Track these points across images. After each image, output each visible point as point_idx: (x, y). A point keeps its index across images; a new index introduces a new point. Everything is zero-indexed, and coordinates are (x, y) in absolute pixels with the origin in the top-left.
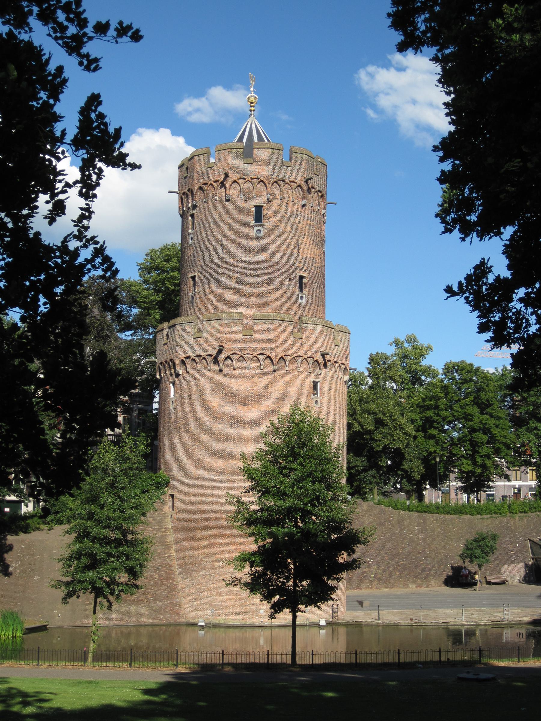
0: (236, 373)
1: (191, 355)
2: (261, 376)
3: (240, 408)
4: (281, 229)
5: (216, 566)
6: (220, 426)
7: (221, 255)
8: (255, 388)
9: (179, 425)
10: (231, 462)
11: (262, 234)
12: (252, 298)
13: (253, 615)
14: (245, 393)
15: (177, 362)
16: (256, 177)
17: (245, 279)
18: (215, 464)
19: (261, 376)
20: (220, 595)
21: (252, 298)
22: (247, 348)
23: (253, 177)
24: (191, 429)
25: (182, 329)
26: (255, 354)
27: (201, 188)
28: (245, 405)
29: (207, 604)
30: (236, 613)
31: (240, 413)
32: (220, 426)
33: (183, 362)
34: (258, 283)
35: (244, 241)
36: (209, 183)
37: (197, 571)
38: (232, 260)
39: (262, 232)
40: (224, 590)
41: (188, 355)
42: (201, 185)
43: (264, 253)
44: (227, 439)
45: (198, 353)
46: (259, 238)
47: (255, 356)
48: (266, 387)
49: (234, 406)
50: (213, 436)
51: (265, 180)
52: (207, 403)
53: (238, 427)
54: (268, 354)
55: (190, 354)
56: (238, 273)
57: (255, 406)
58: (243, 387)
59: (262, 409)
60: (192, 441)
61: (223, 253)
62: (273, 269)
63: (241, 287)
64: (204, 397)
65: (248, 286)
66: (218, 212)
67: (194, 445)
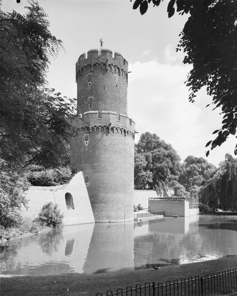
0: (114, 134)
22: (118, 125)
26: (120, 128)
27: (95, 64)
28: (117, 146)
33: (92, 128)
47: (120, 129)
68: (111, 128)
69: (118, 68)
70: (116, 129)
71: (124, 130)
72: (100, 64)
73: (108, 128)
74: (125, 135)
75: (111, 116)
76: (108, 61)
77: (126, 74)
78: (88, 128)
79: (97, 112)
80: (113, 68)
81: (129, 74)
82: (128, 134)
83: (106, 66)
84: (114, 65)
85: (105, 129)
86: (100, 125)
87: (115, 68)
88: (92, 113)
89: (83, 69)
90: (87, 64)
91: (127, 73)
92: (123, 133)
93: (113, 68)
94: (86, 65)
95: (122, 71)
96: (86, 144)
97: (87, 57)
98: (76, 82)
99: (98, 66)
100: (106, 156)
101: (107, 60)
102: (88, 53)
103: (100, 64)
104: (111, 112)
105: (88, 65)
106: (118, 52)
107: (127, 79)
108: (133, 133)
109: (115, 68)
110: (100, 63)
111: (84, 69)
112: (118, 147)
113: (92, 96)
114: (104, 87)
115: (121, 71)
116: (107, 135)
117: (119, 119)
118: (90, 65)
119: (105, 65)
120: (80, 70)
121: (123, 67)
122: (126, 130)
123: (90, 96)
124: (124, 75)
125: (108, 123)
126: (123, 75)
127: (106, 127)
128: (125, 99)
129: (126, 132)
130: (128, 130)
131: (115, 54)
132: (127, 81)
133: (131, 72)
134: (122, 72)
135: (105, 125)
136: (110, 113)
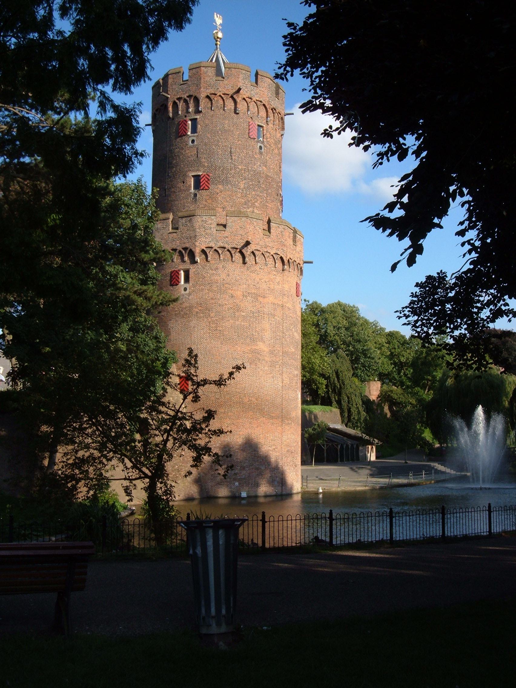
0: (257, 267)
1: (213, 246)
2: (275, 273)
3: (261, 299)
4: (273, 150)
6: (244, 314)
7: (230, 161)
8: (271, 283)
9: (196, 310)
10: (253, 347)
12: (256, 204)
15: (197, 251)
16: (260, 100)
17: (251, 187)
18: (239, 349)
19: (275, 273)
21: (256, 204)
22: (266, 247)
23: (257, 99)
24: (212, 315)
25: (202, 221)
26: (272, 253)
27: (208, 97)
28: (264, 297)
31: (260, 304)
32: (244, 314)
35: (250, 153)
36: (218, 94)
38: (240, 167)
41: (210, 245)
42: (209, 94)
43: (264, 168)
44: (250, 325)
45: (222, 245)
48: (278, 283)
49: (256, 297)
50: (237, 323)
51: (266, 105)
53: (258, 316)
55: (212, 244)
56: (245, 179)
58: (262, 281)
59: (276, 303)
60: (213, 326)
61: (232, 159)
62: (270, 183)
63: (248, 193)
64: (226, 285)
65: (253, 193)
66: (227, 122)
67: (216, 330)
68: (248, 253)
77: (282, 118)
80: (252, 105)
81: (286, 118)
84: (254, 99)
90: (187, 95)
93: (252, 105)
96: (183, 292)
101: (239, 89)
112: (266, 300)
113: (198, 170)
115: (270, 111)
122: (285, 259)
123: (193, 171)
129: (286, 261)
130: (288, 258)
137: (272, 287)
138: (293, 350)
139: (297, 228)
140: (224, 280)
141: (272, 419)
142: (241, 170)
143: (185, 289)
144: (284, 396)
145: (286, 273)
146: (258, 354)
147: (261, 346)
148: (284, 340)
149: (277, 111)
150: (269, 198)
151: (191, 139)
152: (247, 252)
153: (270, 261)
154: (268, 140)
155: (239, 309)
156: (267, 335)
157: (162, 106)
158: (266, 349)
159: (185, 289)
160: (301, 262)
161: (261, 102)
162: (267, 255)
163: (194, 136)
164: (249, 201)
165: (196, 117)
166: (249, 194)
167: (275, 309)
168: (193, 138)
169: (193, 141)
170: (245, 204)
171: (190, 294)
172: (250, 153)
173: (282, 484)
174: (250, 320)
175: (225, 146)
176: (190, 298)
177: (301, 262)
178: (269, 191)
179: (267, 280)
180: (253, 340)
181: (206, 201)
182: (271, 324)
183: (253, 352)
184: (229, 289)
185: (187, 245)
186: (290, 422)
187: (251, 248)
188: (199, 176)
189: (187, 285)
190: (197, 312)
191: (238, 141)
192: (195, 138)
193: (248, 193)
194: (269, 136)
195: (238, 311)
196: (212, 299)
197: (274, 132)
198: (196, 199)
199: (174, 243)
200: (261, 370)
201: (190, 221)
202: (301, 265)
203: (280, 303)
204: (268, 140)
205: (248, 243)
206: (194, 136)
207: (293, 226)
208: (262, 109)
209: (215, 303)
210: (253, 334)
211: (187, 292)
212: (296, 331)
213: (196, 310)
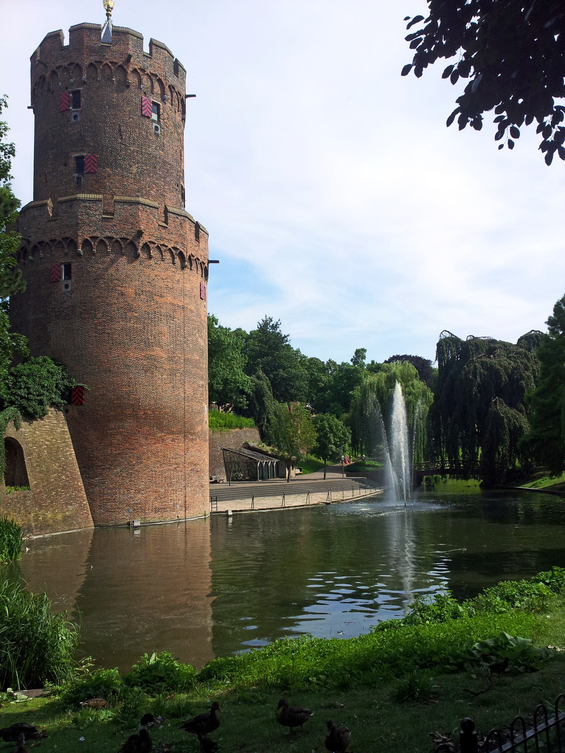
0: (152, 262)
1: (99, 235)
2: (174, 270)
4: (172, 133)
5: (134, 462)
6: (137, 315)
8: (169, 280)
9: (80, 310)
11: (159, 132)
13: (171, 511)
14: (161, 284)
16: (155, 73)
17: (145, 172)
18: (132, 354)
20: (139, 492)
22: (162, 238)
23: (152, 72)
24: (98, 316)
26: (170, 247)
27: (91, 65)
28: (161, 296)
29: (123, 504)
30: (156, 510)
31: (157, 304)
32: (137, 315)
33: (86, 243)
34: (157, 180)
35: (144, 133)
36: (104, 63)
37: (110, 469)
39: (159, 130)
40: (143, 486)
41: (95, 235)
46: (157, 135)
47: (170, 249)
48: (178, 281)
52: (120, 288)
54: (181, 249)
55: (97, 234)
56: (138, 163)
57: (170, 299)
61: (122, 138)
62: (168, 170)
63: (142, 179)
65: (148, 179)
68: (141, 245)
69: (160, 81)
70: (158, 247)
71: (181, 255)
72: (107, 64)
73: (133, 245)
74: (183, 267)
75: (142, 215)
76: (132, 60)
77: (182, 99)
78: (73, 243)
79: (101, 196)
80: (145, 79)
81: (188, 100)
82: (191, 265)
83: (125, 72)
84: (148, 71)
85: (123, 246)
86: (109, 235)
87: (151, 80)
88: (84, 201)
89: (54, 73)
91: (184, 98)
92: (177, 260)
93: (145, 79)
94: (66, 64)
95: (171, 91)
96: (64, 289)
97: (66, 42)
98: (29, 108)
99: (103, 71)
100: (129, 325)
101: (130, 57)
102: (70, 31)
103: (107, 64)
104: (141, 200)
105: (68, 65)
106: (160, 38)
107: (184, 112)
108: (204, 264)
109: (151, 80)
110: (108, 63)
111: (59, 73)
113: (82, 151)
114: (120, 130)
116: (130, 262)
117: (166, 222)
118: (78, 67)
119: (122, 69)
120: (48, 75)
121: (172, 80)
122: (185, 253)
123: (76, 151)
124: (177, 102)
125: (134, 232)
126: (172, 101)
127: (128, 241)
128: (181, 168)
130: (189, 253)
131: (152, 43)
132: (184, 119)
133: (194, 96)
134: (169, 93)
135: (124, 235)
136: (138, 203)
137: (170, 285)
138: (198, 358)
139: (200, 222)
140: (112, 275)
141: (173, 434)
142: (133, 152)
143: (67, 286)
144: (186, 408)
145: (187, 270)
146: (155, 360)
147: (158, 351)
148: (185, 345)
149: (176, 90)
150: (166, 187)
151: (73, 114)
152: (139, 243)
153: (168, 256)
154: (165, 121)
155: (131, 310)
156: (165, 339)
157: (40, 78)
158: (164, 355)
159: (67, 286)
160: (206, 262)
161: (156, 76)
162: (163, 248)
163: (77, 111)
164: (143, 188)
165: (79, 89)
166: (143, 180)
167: (174, 311)
168: (76, 113)
169: (75, 117)
170: (138, 192)
171: (72, 292)
172: (144, 133)
173: (185, 507)
174: (144, 323)
175: (114, 123)
176: (73, 296)
177: (206, 262)
178: (168, 179)
179: (164, 278)
180: (149, 345)
181: (92, 187)
182: (170, 327)
183: (147, 358)
184: (119, 286)
185: (68, 235)
186: (194, 437)
187: (145, 239)
188: (82, 157)
189: (69, 282)
190: (81, 313)
191: (130, 118)
192: (78, 114)
193: (142, 179)
194: (166, 116)
195: (130, 311)
196: (98, 297)
197: (173, 114)
198: (80, 184)
199: (53, 233)
200: (159, 378)
201: (71, 207)
202: (206, 265)
203: (180, 304)
204: (165, 121)
205: (140, 234)
206: (77, 111)
207: (195, 220)
208: (156, 85)
209: (102, 302)
210: (148, 338)
211: (69, 289)
212: (201, 337)
213: (80, 310)
